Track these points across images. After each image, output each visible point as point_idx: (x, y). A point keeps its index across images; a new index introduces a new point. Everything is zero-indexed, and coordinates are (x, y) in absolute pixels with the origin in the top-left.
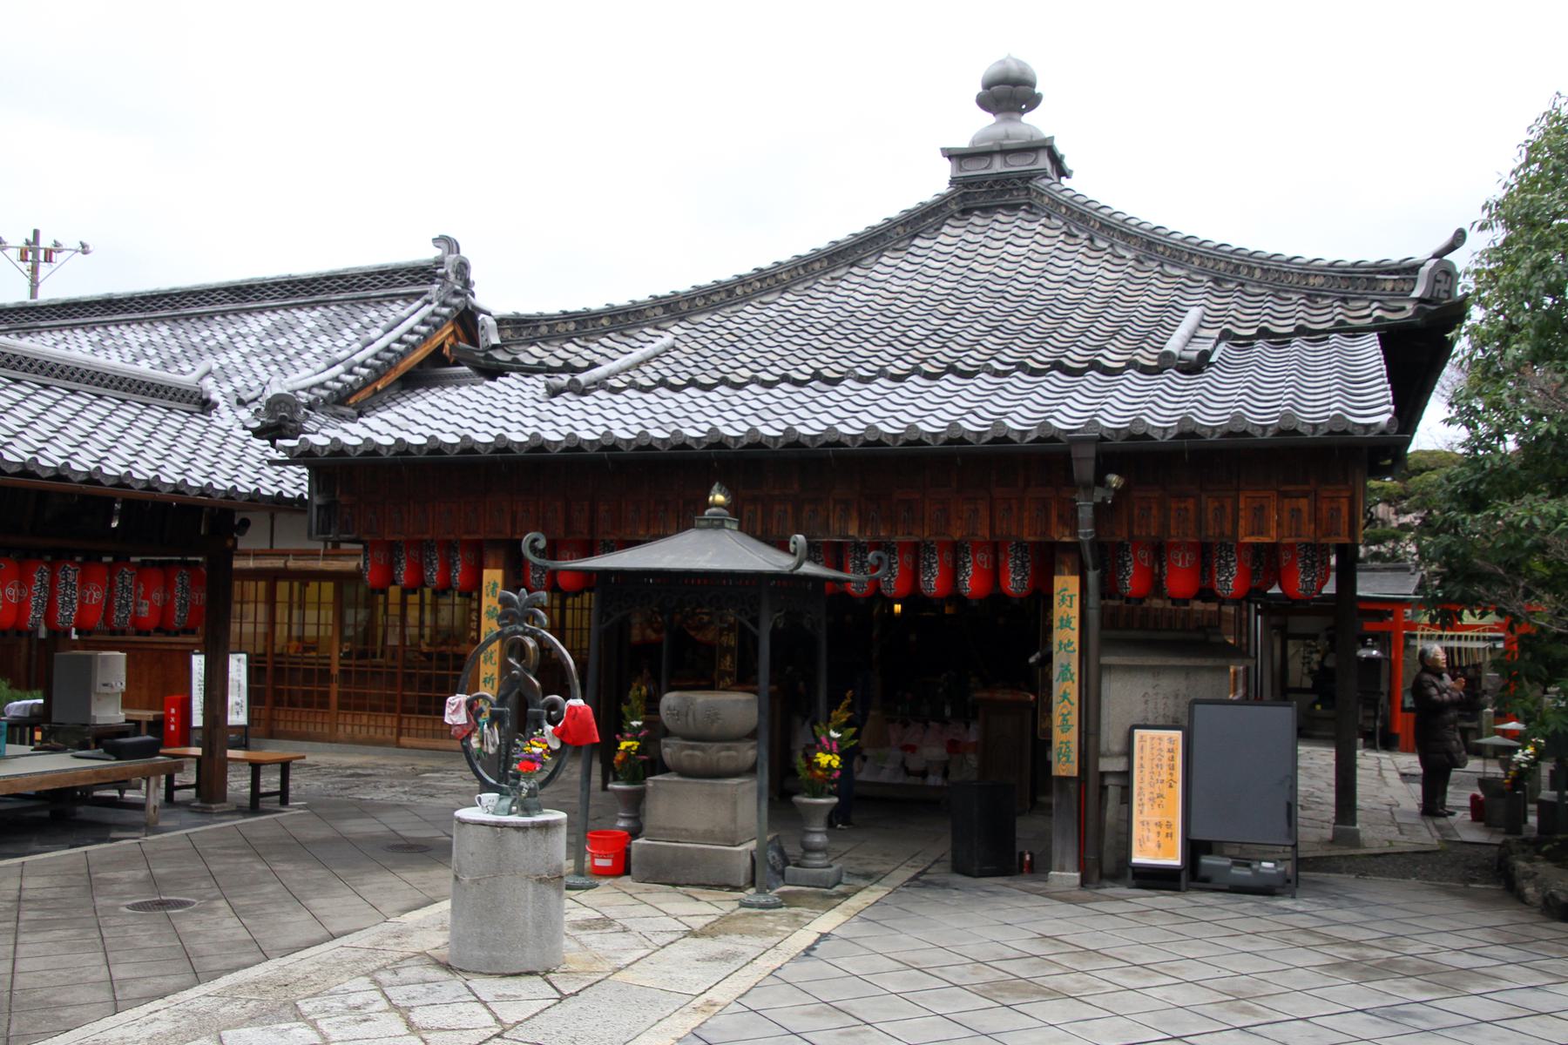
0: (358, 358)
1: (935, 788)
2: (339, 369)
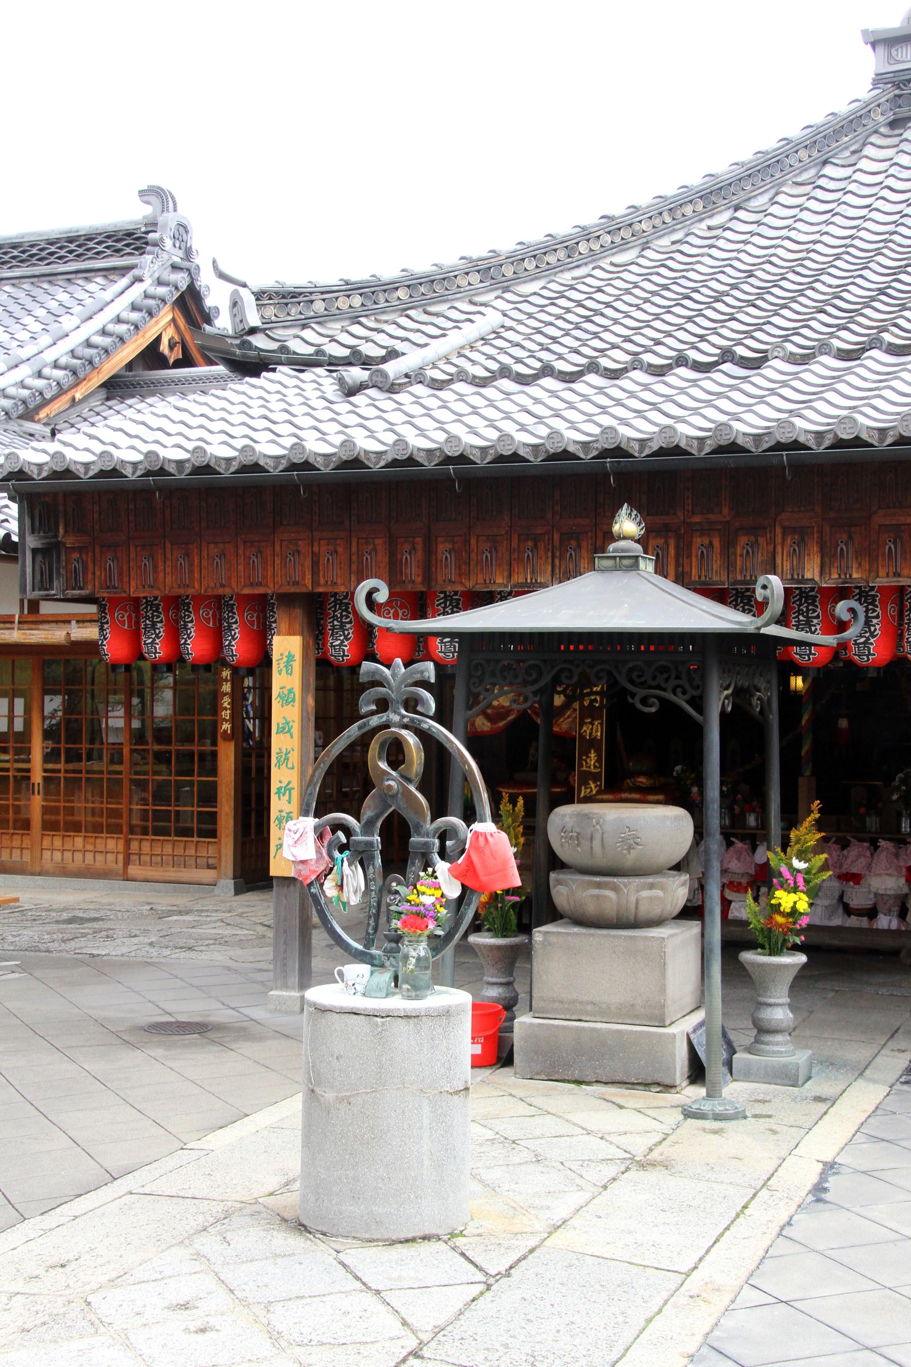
0: (49, 356)
1: (889, 932)
2: (24, 372)
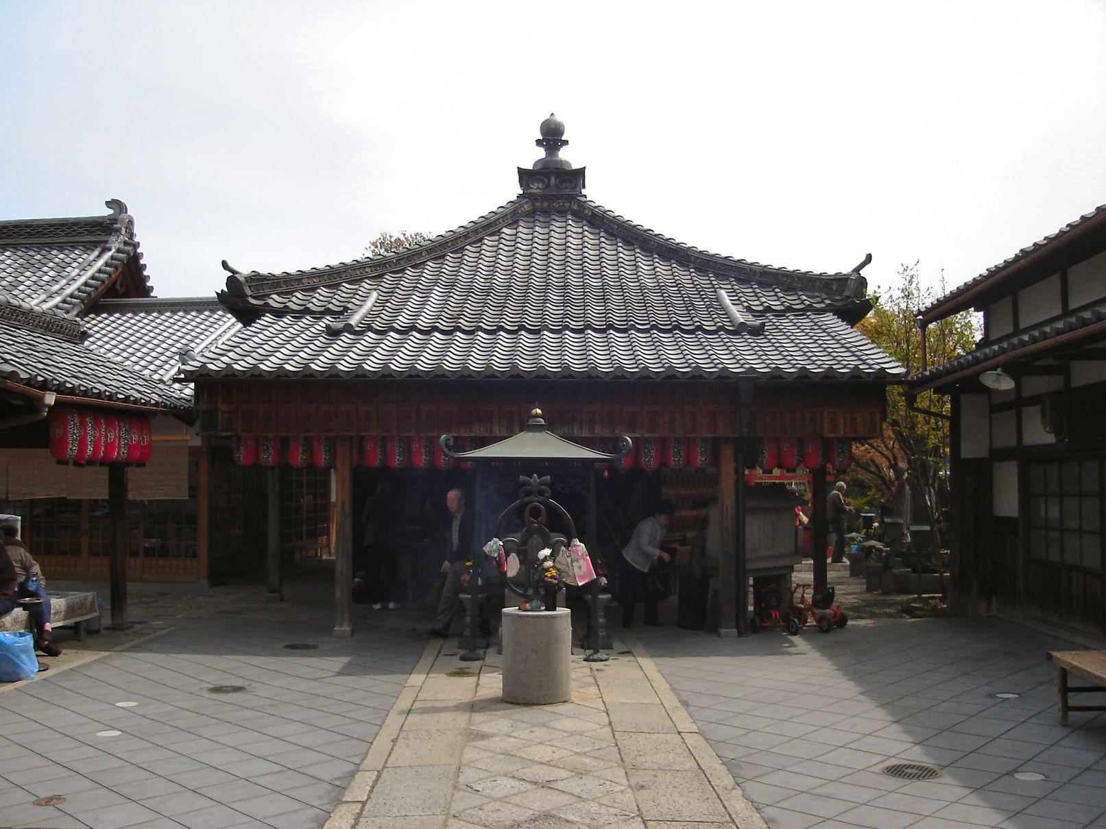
0: (68, 291)
